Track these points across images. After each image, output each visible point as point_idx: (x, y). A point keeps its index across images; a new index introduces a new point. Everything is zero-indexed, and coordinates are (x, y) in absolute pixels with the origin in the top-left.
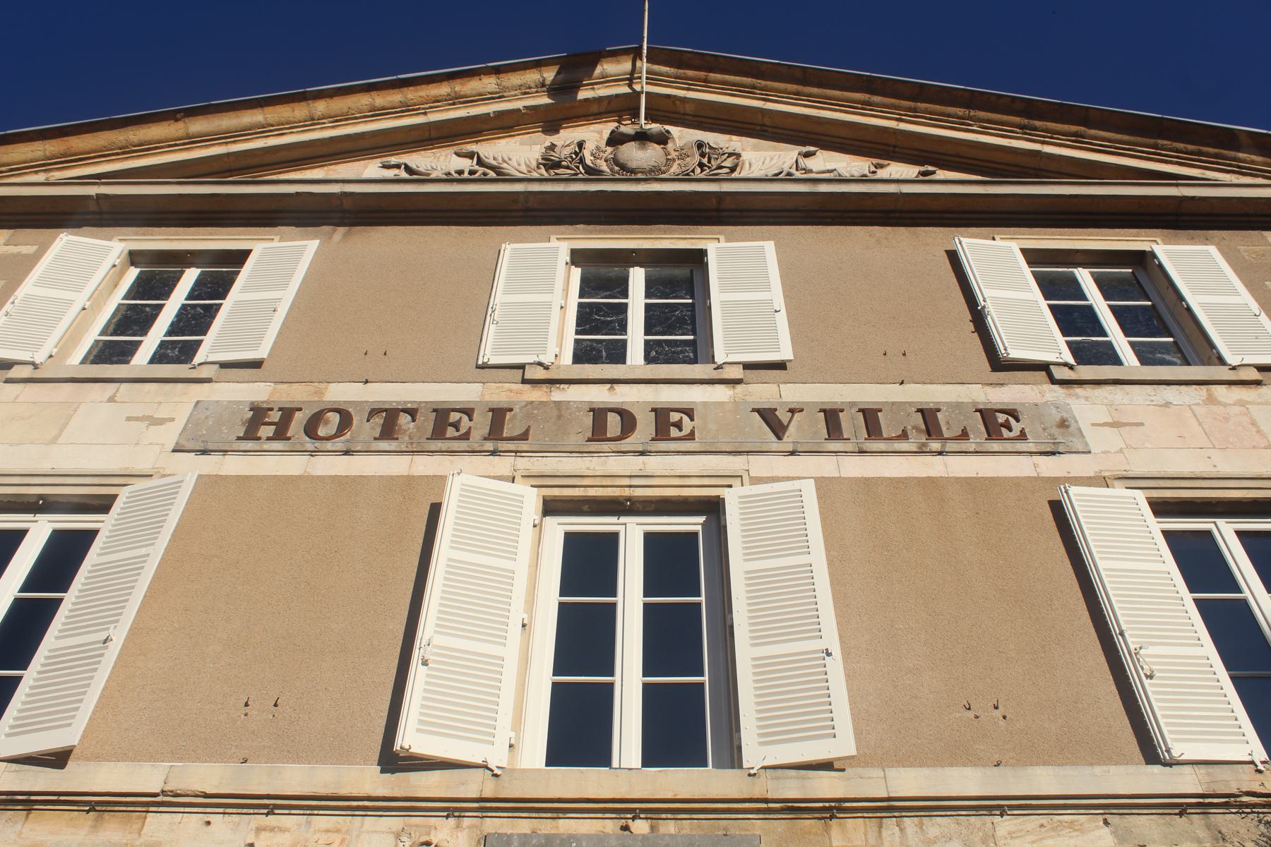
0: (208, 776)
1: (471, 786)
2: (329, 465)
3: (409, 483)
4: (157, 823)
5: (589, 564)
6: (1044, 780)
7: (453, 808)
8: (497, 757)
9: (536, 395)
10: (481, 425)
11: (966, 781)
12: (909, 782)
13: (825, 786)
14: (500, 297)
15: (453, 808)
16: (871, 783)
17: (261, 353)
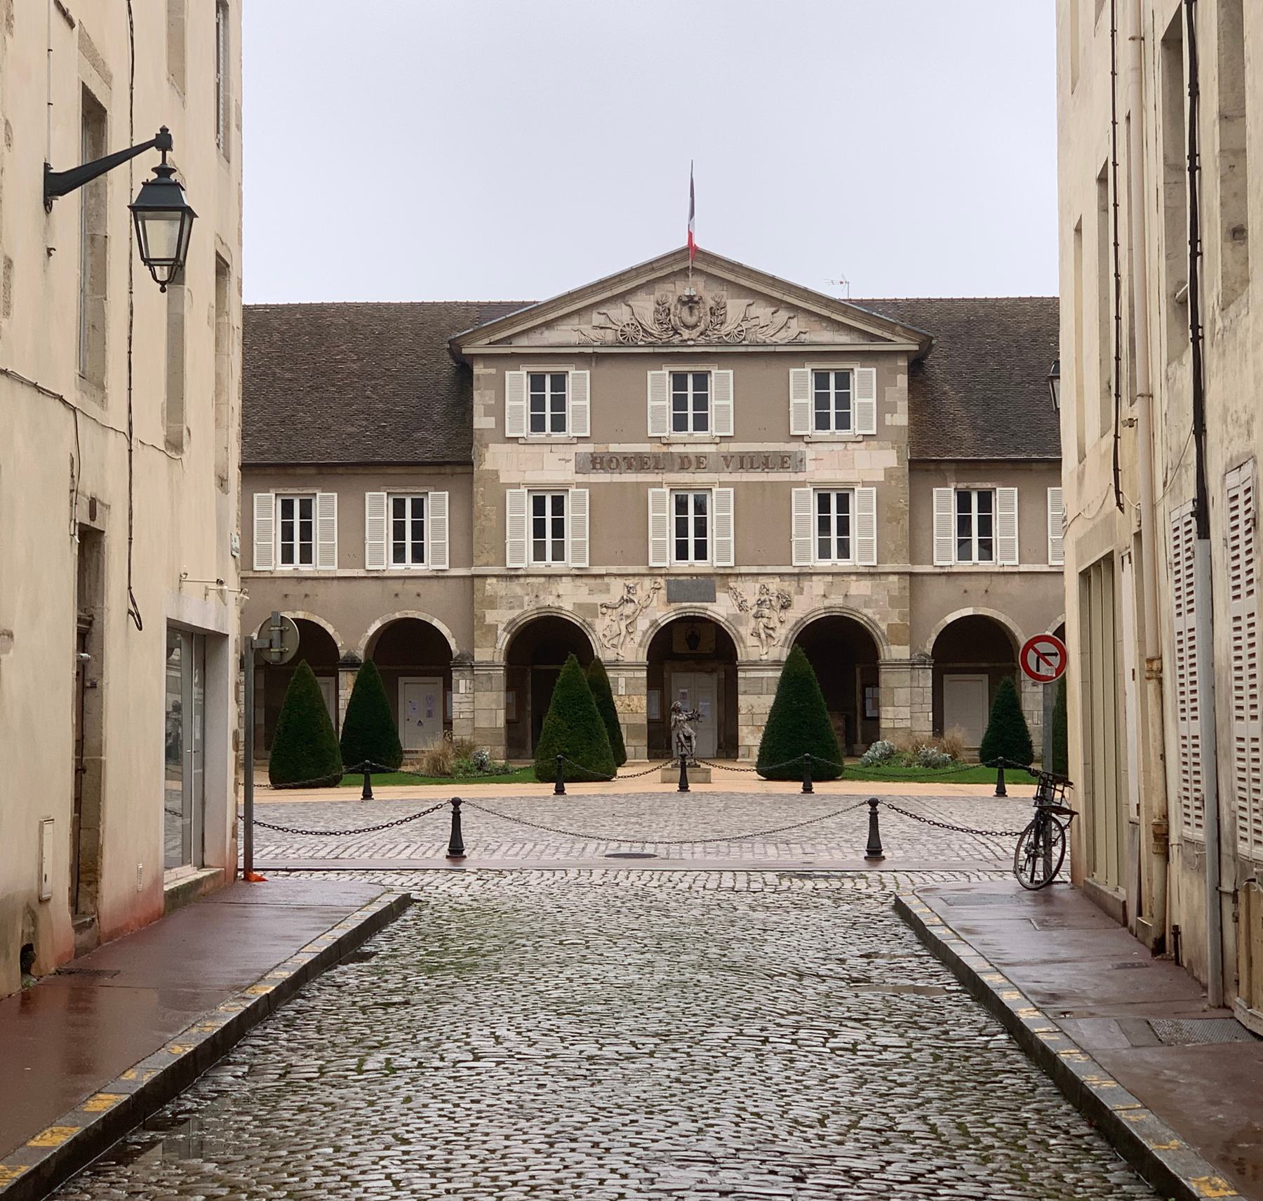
0: (614, 569)
1: (663, 571)
2: (617, 478)
3: (638, 484)
4: (606, 579)
5: (681, 506)
6: (769, 569)
7: (661, 575)
8: (667, 564)
9: (665, 449)
10: (651, 463)
11: (754, 570)
12: (744, 570)
13: (728, 571)
14: (650, 403)
15: (661, 575)
16: (737, 571)
17: (588, 434)
